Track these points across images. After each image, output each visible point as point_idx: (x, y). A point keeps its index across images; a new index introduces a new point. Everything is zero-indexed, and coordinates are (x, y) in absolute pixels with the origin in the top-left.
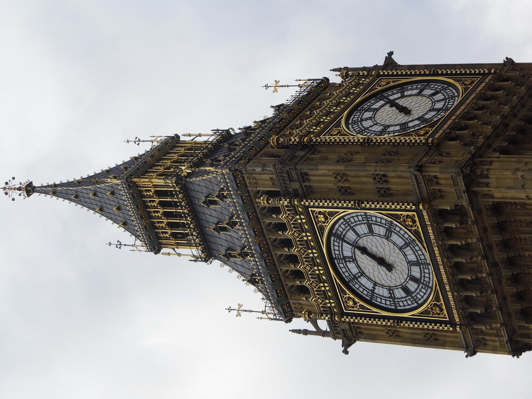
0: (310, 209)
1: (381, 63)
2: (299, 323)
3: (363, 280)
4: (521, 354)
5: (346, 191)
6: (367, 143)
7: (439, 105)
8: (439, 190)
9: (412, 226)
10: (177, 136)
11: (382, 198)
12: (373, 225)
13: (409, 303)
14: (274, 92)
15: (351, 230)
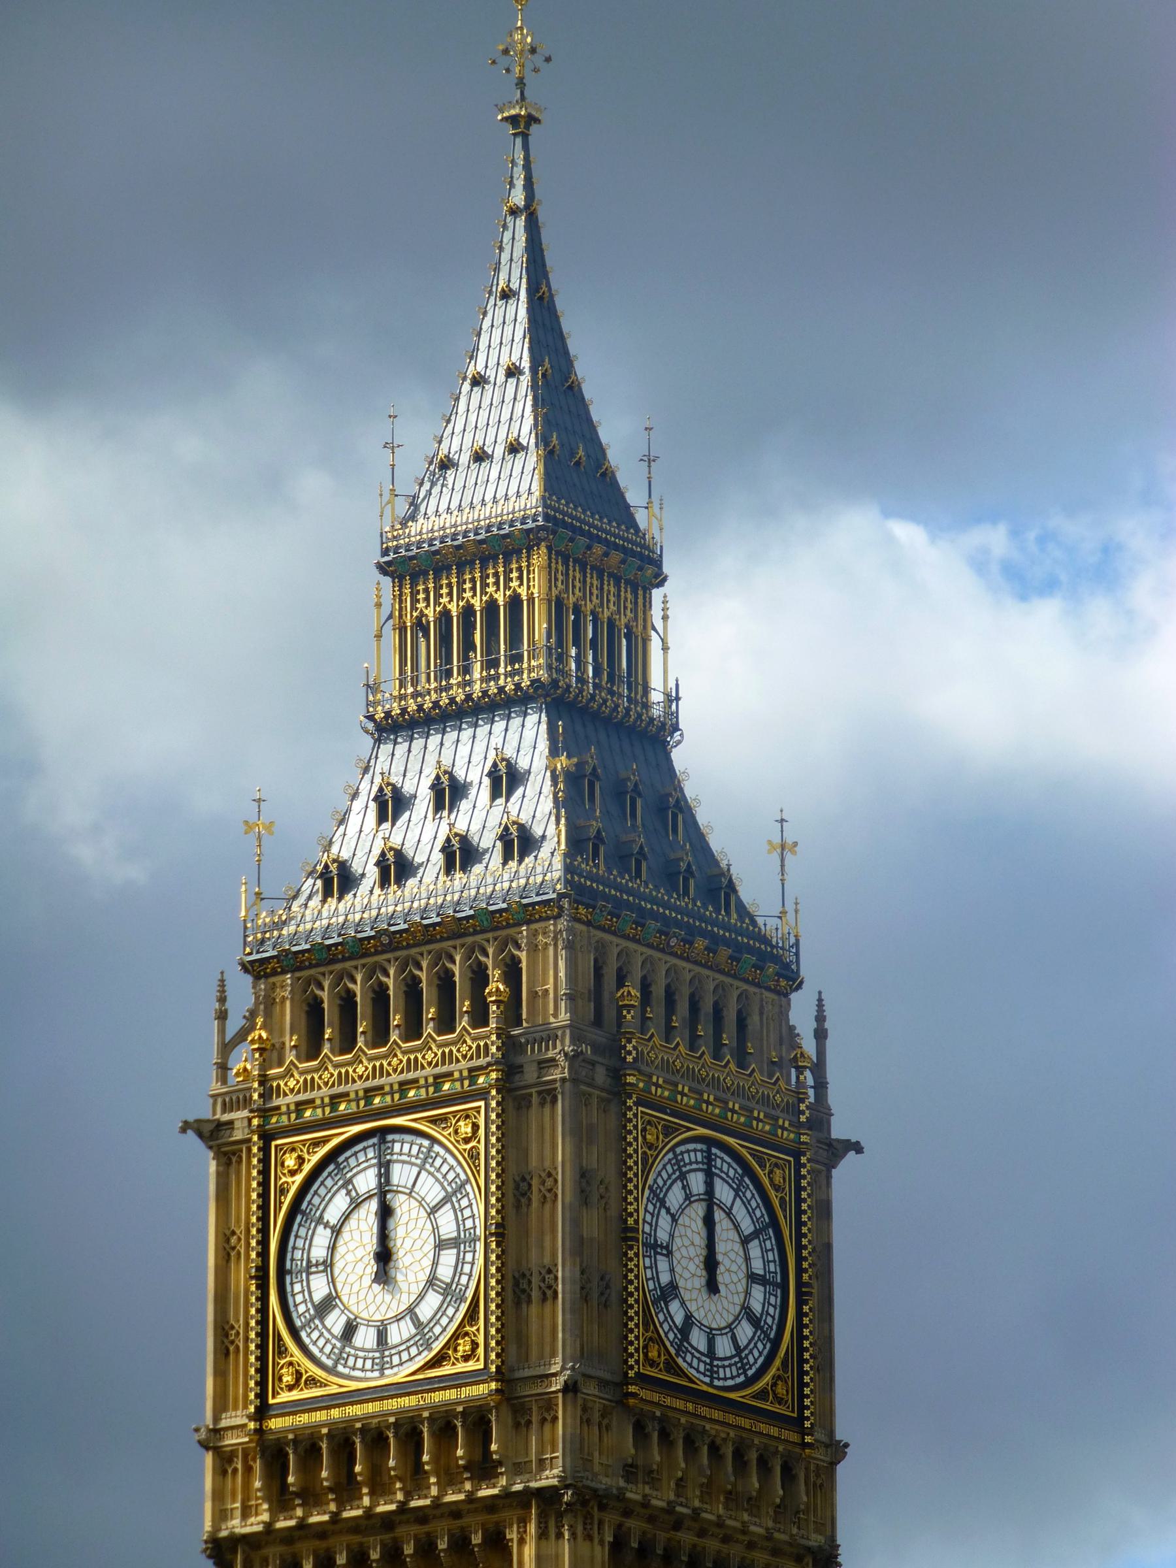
0: (482, 1103)
1: (839, 1130)
2: (243, 993)
3: (340, 1203)
4: (210, 1557)
5: (524, 1195)
6: (627, 1235)
7: (724, 1347)
8: (529, 1422)
9: (455, 1350)
10: (661, 584)
11: (509, 1284)
12: (455, 1251)
13: (302, 1310)
14: (770, 842)
15: (443, 1194)
